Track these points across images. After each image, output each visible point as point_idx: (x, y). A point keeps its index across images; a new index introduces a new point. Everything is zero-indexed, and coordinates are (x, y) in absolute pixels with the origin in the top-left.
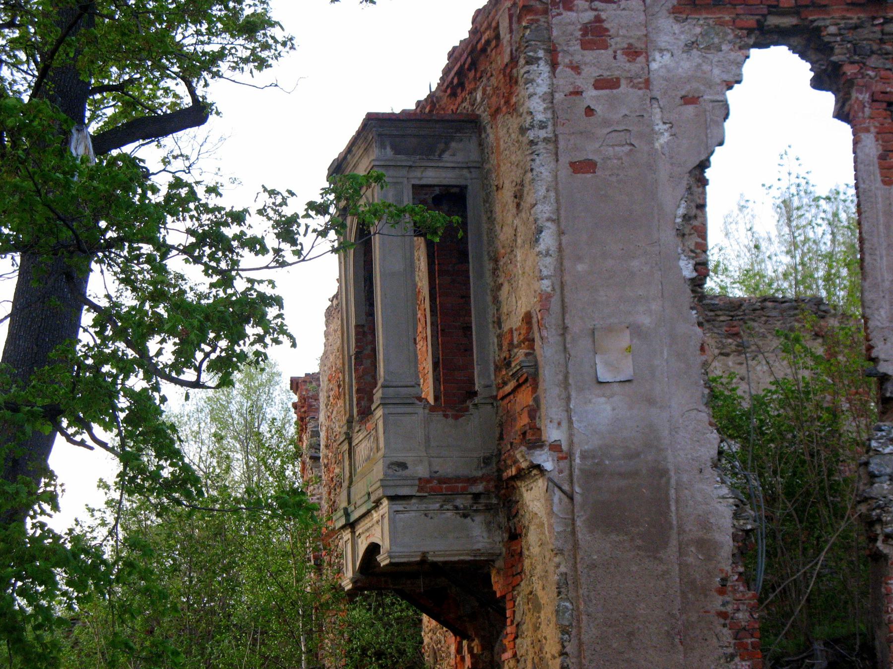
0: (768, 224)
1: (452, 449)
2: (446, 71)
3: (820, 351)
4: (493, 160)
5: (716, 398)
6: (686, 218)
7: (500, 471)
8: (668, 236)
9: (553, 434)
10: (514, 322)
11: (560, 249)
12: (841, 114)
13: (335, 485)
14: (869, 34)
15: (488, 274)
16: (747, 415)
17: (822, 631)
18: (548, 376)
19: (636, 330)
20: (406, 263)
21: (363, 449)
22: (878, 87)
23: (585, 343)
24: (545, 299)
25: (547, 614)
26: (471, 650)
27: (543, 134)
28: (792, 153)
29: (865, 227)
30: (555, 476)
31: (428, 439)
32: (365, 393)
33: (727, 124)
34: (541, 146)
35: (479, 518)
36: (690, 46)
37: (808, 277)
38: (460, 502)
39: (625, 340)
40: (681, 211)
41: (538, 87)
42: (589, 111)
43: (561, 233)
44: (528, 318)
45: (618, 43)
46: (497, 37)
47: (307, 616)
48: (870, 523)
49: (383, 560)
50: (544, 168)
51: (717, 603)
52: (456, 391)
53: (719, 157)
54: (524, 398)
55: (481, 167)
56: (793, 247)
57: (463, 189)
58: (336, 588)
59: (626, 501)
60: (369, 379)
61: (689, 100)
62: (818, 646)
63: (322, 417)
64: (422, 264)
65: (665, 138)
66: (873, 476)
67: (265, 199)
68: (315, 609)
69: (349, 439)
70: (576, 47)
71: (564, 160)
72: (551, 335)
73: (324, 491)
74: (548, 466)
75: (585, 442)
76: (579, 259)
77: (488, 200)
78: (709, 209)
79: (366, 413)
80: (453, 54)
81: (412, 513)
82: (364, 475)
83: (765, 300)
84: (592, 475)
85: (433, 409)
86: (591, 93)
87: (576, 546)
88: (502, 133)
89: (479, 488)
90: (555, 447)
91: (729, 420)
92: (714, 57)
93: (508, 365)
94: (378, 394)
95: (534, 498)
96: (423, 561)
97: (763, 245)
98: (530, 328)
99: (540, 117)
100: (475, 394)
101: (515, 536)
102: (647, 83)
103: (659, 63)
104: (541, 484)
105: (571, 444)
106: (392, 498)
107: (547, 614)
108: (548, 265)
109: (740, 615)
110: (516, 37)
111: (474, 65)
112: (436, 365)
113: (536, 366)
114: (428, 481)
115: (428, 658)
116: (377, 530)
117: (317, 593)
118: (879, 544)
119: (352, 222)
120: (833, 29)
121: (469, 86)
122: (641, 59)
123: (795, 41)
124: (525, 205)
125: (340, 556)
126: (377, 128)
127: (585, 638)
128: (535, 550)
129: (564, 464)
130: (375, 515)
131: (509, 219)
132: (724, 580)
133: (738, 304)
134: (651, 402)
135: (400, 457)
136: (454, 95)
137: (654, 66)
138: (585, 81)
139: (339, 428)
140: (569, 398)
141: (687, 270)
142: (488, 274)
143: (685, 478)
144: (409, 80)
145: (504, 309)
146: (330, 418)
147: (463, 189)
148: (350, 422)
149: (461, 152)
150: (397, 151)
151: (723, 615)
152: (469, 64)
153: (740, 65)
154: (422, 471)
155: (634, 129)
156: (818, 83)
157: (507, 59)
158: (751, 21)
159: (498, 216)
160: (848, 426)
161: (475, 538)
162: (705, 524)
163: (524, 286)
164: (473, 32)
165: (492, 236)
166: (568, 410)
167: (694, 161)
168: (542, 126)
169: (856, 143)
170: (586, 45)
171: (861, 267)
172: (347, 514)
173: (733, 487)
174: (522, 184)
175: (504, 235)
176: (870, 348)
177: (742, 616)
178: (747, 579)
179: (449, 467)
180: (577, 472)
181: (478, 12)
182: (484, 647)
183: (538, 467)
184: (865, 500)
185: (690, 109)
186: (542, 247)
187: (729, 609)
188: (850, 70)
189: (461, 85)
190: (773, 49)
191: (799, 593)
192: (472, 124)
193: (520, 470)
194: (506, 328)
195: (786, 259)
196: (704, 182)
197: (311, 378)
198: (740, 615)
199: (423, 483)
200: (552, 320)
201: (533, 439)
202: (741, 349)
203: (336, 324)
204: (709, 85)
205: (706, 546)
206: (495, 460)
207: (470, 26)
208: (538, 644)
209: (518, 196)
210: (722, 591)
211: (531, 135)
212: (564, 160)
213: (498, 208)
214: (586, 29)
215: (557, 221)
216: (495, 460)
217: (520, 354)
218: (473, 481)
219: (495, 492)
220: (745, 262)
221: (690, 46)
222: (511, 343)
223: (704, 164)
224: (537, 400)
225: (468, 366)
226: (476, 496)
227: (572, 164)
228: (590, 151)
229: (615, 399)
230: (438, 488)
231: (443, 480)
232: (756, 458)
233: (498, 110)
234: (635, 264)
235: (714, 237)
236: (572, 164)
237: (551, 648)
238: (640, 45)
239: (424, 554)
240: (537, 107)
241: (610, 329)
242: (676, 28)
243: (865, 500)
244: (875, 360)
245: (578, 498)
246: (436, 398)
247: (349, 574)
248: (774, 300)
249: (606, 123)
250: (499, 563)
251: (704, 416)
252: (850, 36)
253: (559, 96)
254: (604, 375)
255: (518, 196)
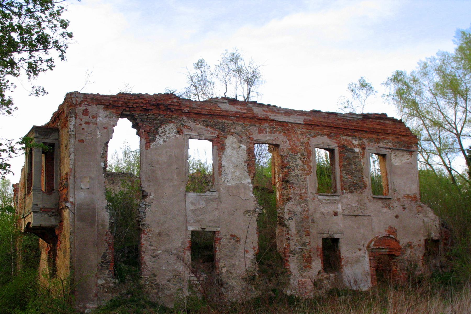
0: (121, 156)
1: (49, 202)
2: (52, 118)
3: (130, 184)
4: (61, 138)
5: (107, 193)
6: (103, 154)
7: (59, 207)
8: (99, 157)
9: (71, 199)
10: (64, 174)
11: (75, 159)
12: (138, 134)
13: (21, 209)
14: (145, 117)
15: (58, 164)
16: (114, 198)
17: (127, 244)
18: (71, 186)
19: (90, 178)
20: (40, 160)
21: (28, 200)
22: (146, 129)
23: (79, 180)
24: (71, 170)
25: (67, 239)
26: (50, 246)
27: (73, 133)
28: (126, 141)
29: (141, 158)
30: (71, 209)
31: (43, 199)
32: (29, 188)
33: (113, 134)
34: (72, 136)
35: (53, 217)
36: (106, 117)
37: (129, 168)
38: (49, 213)
39: (88, 179)
40: (102, 152)
41: (72, 122)
42: (83, 129)
43: (75, 155)
44: (67, 174)
45: (90, 114)
46: (64, 111)
47: (13, 238)
48: (139, 222)
49: (31, 226)
50: (72, 141)
51: (105, 238)
52: (50, 189)
53: (111, 141)
54: (65, 191)
55: (58, 140)
56: (126, 162)
57: (54, 144)
58: (21, 232)
59: (86, 215)
60: (30, 185)
61: (105, 128)
62: (126, 248)
63: (19, 193)
64: (44, 160)
65: (99, 136)
66: (140, 212)
67: (7, 142)
68: (15, 237)
69: (25, 198)
70: (81, 115)
71: (77, 139)
72: (72, 178)
73: (19, 210)
74: (69, 206)
75: (78, 201)
76: (79, 161)
77: (60, 148)
78: (108, 152)
79: (29, 193)
80: (54, 114)
81: (38, 216)
82: (28, 206)
83: (119, 173)
84: (79, 209)
85: (44, 193)
86: (84, 125)
87: (75, 223)
88: (63, 132)
89: (54, 211)
90: (71, 202)
91: (110, 199)
92: (112, 119)
93: (62, 184)
94: (32, 189)
95: (66, 213)
96: (40, 226)
97: (120, 161)
98: (67, 176)
99: (72, 129)
100: (54, 190)
101: (61, 222)
102: (96, 123)
103: (99, 120)
104: (68, 210)
105: (75, 202)
106: (34, 212)
107: (67, 239)
108: (72, 162)
109: (110, 241)
110: (68, 111)
111: (58, 117)
112: (45, 183)
113: (68, 184)
114: (42, 208)
115: (40, 248)
116: (30, 219)
117: (16, 232)
118: (140, 226)
119: (28, 149)
120: (137, 116)
121: (57, 121)
122: (95, 118)
123: (129, 117)
124: (68, 149)
125: (22, 224)
126: (35, 129)
127: (76, 244)
128: (66, 225)
129: (73, 206)
130: (30, 216)
131: (64, 151)
132: (107, 233)
133: (113, 174)
134: (93, 193)
135: (36, 203)
136: (53, 123)
137: (98, 120)
138: (83, 122)
139: (23, 196)
140: (75, 192)
141: (103, 165)
142: (58, 164)
143: (99, 210)
144: (43, 119)
145: (62, 171)
146: (21, 193)
147: (54, 144)
148: (25, 195)
149: (54, 136)
150: (39, 134)
151: (106, 240)
152: (57, 116)
153: (117, 122)
154: (41, 206)
155: (93, 134)
156: (133, 127)
157: (66, 116)
158: (120, 112)
159: (61, 150)
160: (135, 202)
161: (52, 222)
162: (103, 221)
163: (66, 166)
164: (58, 109)
165: (60, 155)
166: (74, 194)
167: (105, 142)
168: (73, 131)
169: (140, 140)
170: (83, 114)
171: (140, 167)
172: (23, 215)
173: (110, 213)
174: (67, 144)
175: (62, 155)
176: (141, 184)
177: (110, 241)
178: (112, 233)
179: (47, 206)
180: (76, 208)
181: (60, 105)
182: (53, 246)
183: (67, 207)
184: (138, 217)
185: (105, 130)
186: (71, 158)
187: (107, 239)
188: (140, 125)
189: (55, 121)
190: (124, 119)
191: (123, 236)
192: (57, 130)
193: (63, 207)
194: (62, 175)
195: (124, 164)
196: (107, 146)
197: (17, 184)
198: (110, 241)
199: (41, 209)
200: (72, 175)
201: (66, 200)
202: (113, 183)
203: (23, 173)
204: (110, 125)
205: (103, 226)
206: (58, 204)
207: (58, 108)
208: (65, 246)
209: (66, 146)
210: (106, 235)
211: (70, 133)
212: (77, 139)
213: (61, 149)
214: (84, 111)
215: (74, 152)
216: (58, 204)
217: (65, 181)
218: (52, 209)
219: (57, 212)
220: (116, 164)
221: (106, 117)
222: (63, 179)
223: (108, 142)
224: (68, 192)
225: (53, 184)
226: (53, 212)
227: (79, 140)
228: (83, 138)
229: (85, 192)
230: (44, 210)
231: (46, 208)
232: (115, 206)
233: (63, 127)
234: (91, 163)
235: (109, 158)
236: (79, 140)
237: (68, 246)
238: (95, 115)
239: (41, 225)
240: (72, 127)
241: (85, 177)
242: (104, 112)
243: (138, 217)
244: (141, 187)
245: (76, 214)
246: (45, 190)
247: (23, 228)
248: (121, 173)
249: (87, 132)
250: (57, 227)
251: (104, 197)
252: (140, 117)
253: (77, 125)
254: (83, 187)
255: (66, 146)
